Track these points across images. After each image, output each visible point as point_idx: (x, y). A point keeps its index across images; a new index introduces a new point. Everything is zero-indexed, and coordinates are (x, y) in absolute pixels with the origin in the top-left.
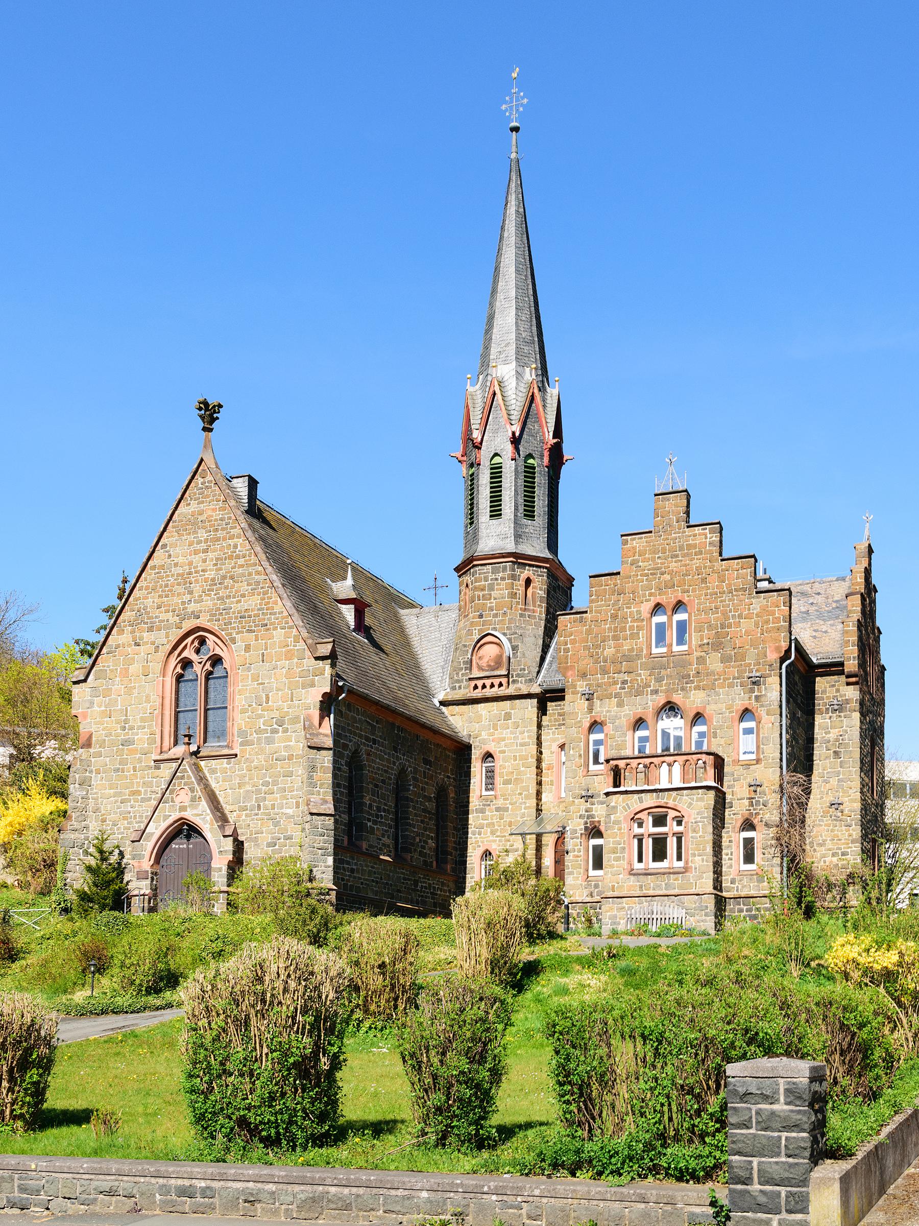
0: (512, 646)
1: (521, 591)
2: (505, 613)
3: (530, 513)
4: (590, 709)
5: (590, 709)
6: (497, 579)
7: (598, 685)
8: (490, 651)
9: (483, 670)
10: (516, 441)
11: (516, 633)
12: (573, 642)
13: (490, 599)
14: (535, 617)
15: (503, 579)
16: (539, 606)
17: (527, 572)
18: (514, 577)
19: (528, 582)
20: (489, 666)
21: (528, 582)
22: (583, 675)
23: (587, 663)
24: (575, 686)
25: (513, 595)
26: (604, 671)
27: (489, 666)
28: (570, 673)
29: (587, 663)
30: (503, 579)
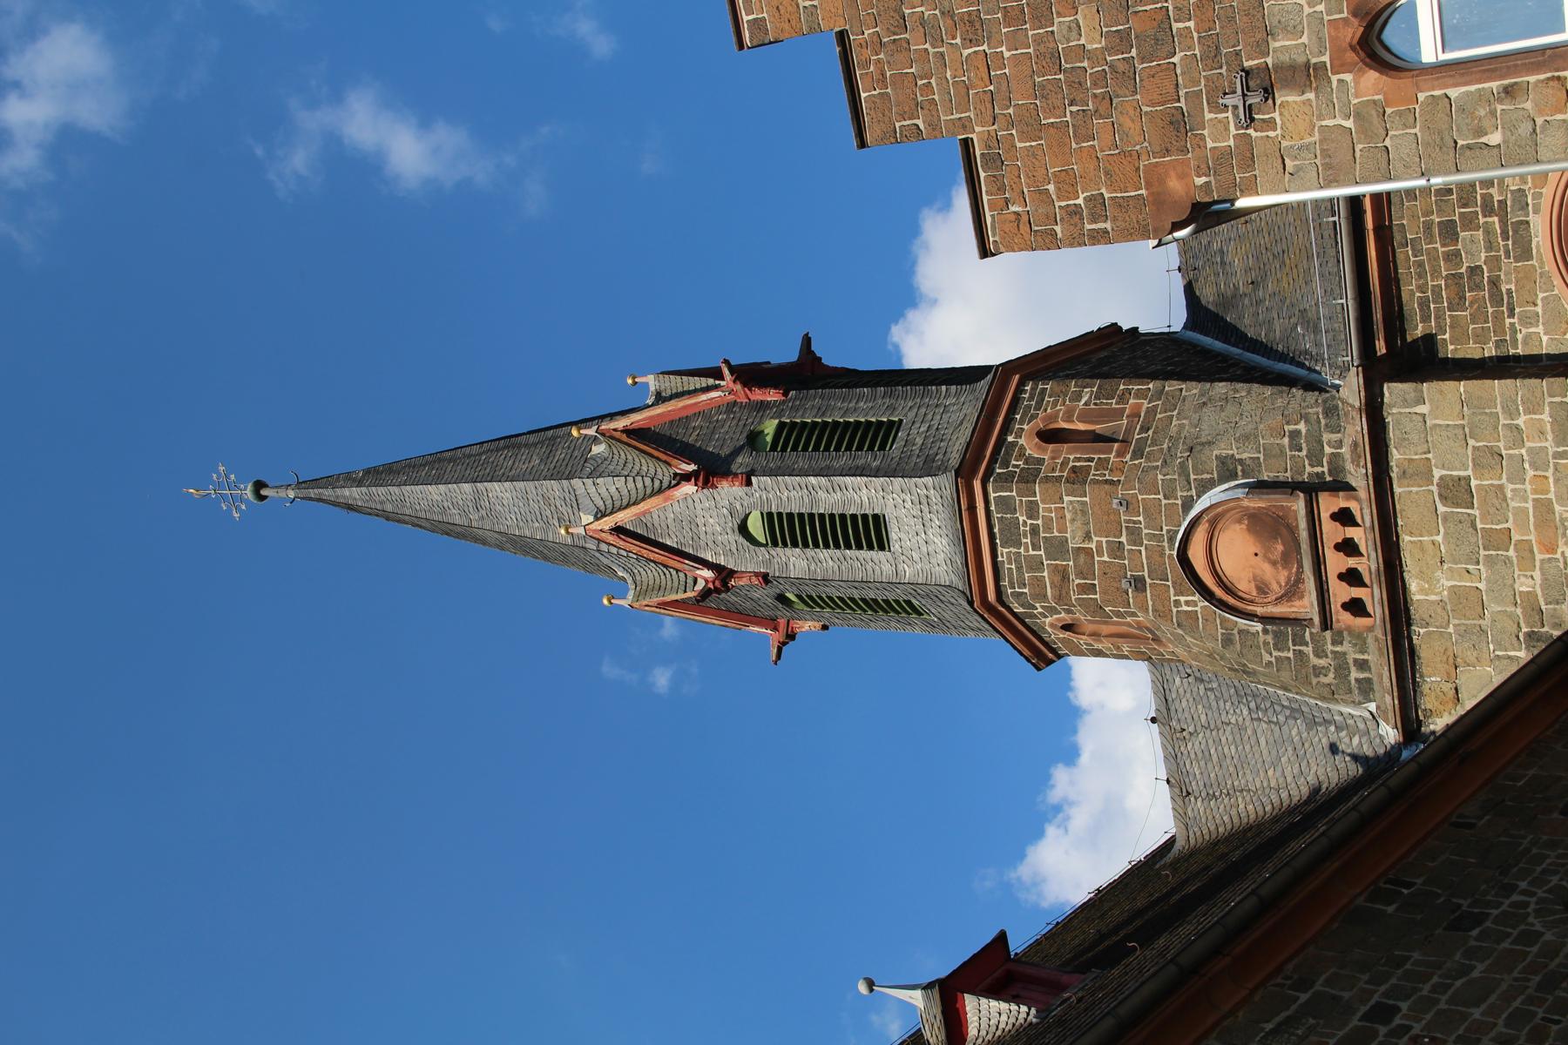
0: (1222, 480)
1: (1071, 455)
2: (1127, 504)
3: (878, 435)
4: (1307, 75)
5: (1307, 75)
6: (1034, 531)
7: (1213, 55)
8: (1239, 556)
9: (1299, 580)
10: (711, 470)
11: (1183, 466)
12: (1068, 183)
13: (1089, 552)
14: (1152, 412)
15: (1032, 511)
16: (1123, 399)
17: (1025, 440)
18: (1029, 477)
19: (1050, 436)
20: (1286, 559)
21: (1050, 436)
22: (1180, 126)
23: (1135, 117)
24: (1224, 156)
25: (1078, 477)
26: (1161, 38)
27: (1286, 559)
28: (1174, 185)
29: (1135, 117)
30: (1032, 511)
